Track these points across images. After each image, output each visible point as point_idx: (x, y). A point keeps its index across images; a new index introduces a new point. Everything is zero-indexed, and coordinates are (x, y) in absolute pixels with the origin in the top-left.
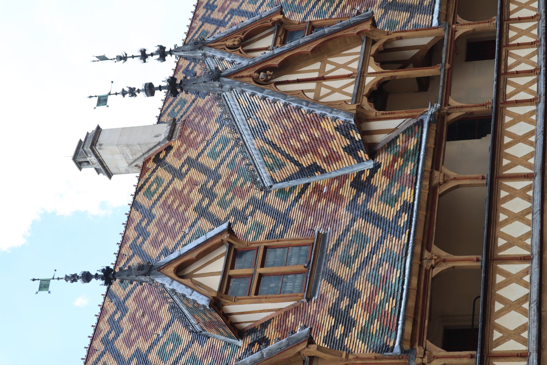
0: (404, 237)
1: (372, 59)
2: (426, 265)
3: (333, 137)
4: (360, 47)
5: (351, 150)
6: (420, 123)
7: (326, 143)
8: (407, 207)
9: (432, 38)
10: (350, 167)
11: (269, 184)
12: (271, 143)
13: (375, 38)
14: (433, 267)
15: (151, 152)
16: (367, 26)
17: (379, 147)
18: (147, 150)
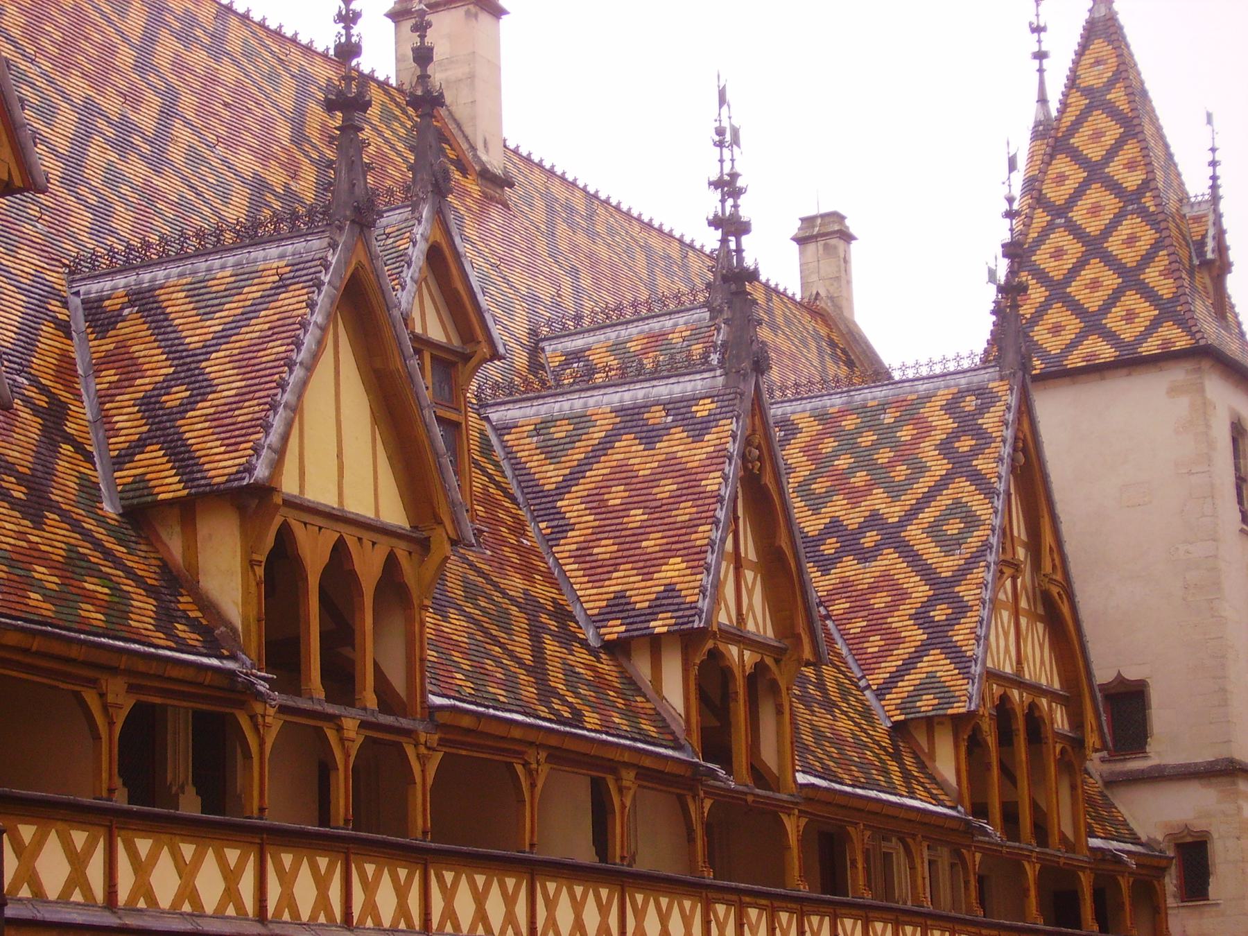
0: (543, 711)
1: (758, 658)
2: (531, 755)
3: (647, 577)
4: (770, 633)
5: (619, 605)
6: (678, 747)
7: (627, 559)
8: (577, 719)
9: (774, 769)
11: (494, 417)
12: (605, 446)
13: (783, 663)
14: (526, 764)
15: (452, 126)
16: (807, 654)
17: (625, 664)
18: (457, 116)
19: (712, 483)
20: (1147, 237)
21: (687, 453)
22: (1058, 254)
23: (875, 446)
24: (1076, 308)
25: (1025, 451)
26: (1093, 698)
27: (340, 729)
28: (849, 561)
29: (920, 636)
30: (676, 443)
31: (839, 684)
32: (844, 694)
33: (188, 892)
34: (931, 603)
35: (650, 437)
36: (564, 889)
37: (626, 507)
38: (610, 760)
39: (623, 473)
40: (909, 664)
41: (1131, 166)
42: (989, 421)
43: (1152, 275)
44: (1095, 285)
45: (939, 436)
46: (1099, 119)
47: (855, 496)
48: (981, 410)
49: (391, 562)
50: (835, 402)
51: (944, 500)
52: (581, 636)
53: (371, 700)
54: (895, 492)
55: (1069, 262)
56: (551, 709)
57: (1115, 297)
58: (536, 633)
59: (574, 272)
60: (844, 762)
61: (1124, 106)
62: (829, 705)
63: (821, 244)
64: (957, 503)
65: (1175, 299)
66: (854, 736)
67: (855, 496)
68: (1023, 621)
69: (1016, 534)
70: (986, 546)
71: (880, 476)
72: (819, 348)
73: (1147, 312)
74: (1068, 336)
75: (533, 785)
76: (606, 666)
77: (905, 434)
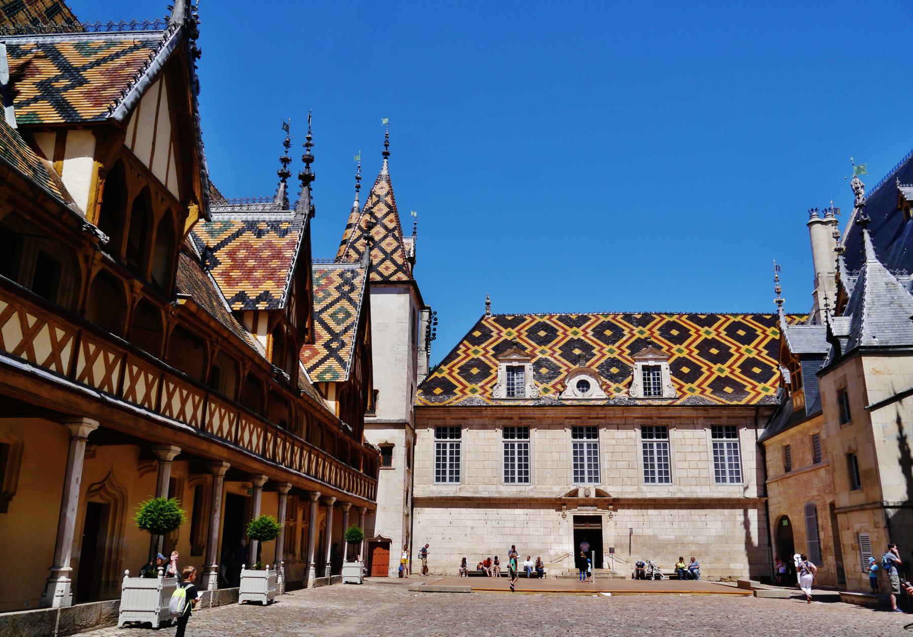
5: (241, 297)
7: (247, 279)
10: (226, 292)
12: (239, 234)
14: (211, 342)
20: (395, 244)
27: (132, 287)
29: (326, 352)
30: (272, 237)
33: (26, 345)
34: (331, 341)
35: (260, 234)
37: (246, 258)
38: (244, 354)
39: (247, 246)
41: (391, 221)
42: (356, 282)
43: (396, 256)
45: (336, 284)
46: (382, 205)
48: (353, 278)
49: (168, 212)
51: (337, 306)
53: (149, 280)
57: (383, 261)
61: (390, 202)
64: (342, 307)
65: (404, 264)
70: (353, 324)
73: (393, 268)
75: (213, 353)
77: (323, 282)
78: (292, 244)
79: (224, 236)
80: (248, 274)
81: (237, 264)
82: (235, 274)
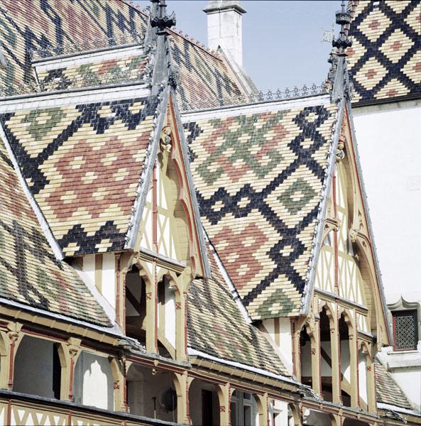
0: (21, 298)
1: (165, 272)
3: (95, 215)
4: (175, 258)
5: (76, 234)
7: (81, 204)
8: (44, 304)
10: (53, 228)
19: (138, 157)
21: (124, 137)
22: (374, 25)
23: (249, 144)
24: (383, 59)
25: (344, 149)
26: (384, 312)
28: (229, 216)
29: (273, 265)
30: (117, 129)
31: (219, 294)
32: (222, 300)
34: (281, 245)
35: (101, 125)
36: (30, 414)
37: (84, 169)
39: (83, 149)
40: (265, 283)
42: (323, 129)
44: (397, 46)
45: (291, 138)
47: (235, 175)
48: (319, 122)
50: (223, 115)
51: (292, 179)
52: (50, 252)
54: (261, 174)
55: (381, 30)
56: (27, 297)
58: (20, 248)
59: (57, 21)
60: (220, 342)
62: (212, 307)
63: (222, 14)
66: (227, 327)
67: (235, 175)
68: (340, 259)
69: (337, 203)
71: (252, 163)
72: (218, 81)
74: (378, 79)
76: (68, 271)
77: (269, 136)
78: (145, 141)
79: (52, 135)
80: (84, 197)
81: (73, 181)
82: (68, 197)
